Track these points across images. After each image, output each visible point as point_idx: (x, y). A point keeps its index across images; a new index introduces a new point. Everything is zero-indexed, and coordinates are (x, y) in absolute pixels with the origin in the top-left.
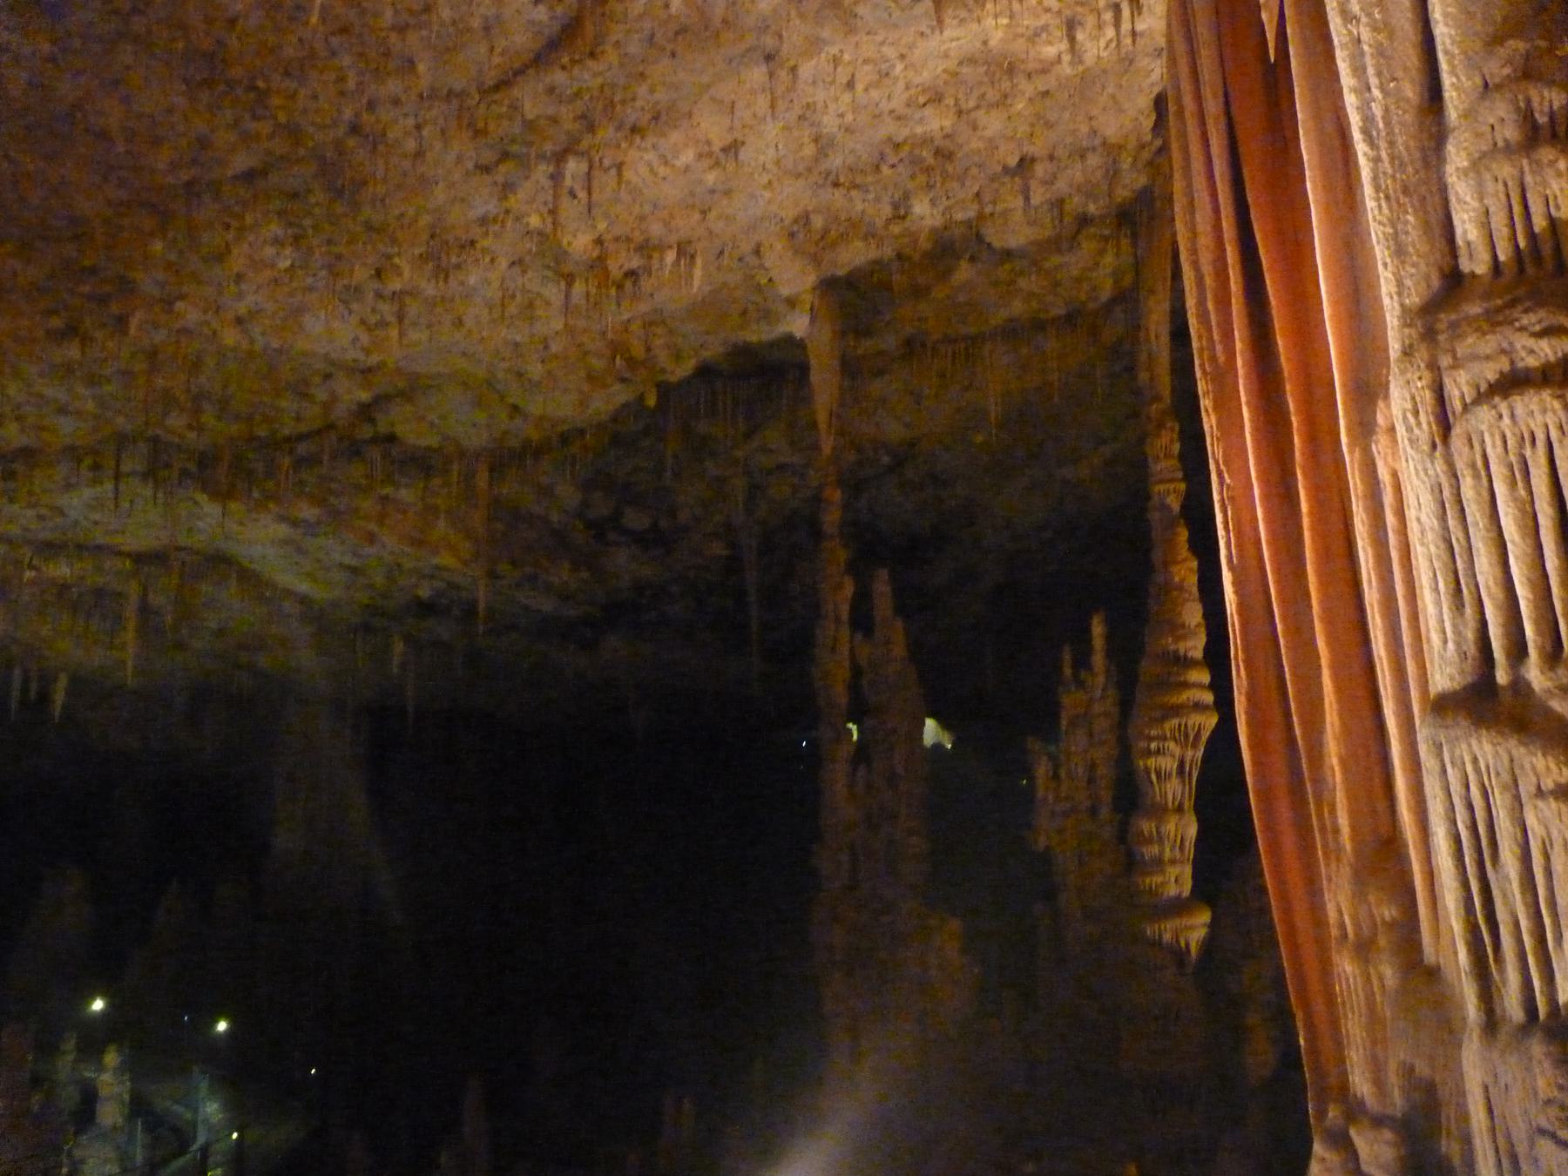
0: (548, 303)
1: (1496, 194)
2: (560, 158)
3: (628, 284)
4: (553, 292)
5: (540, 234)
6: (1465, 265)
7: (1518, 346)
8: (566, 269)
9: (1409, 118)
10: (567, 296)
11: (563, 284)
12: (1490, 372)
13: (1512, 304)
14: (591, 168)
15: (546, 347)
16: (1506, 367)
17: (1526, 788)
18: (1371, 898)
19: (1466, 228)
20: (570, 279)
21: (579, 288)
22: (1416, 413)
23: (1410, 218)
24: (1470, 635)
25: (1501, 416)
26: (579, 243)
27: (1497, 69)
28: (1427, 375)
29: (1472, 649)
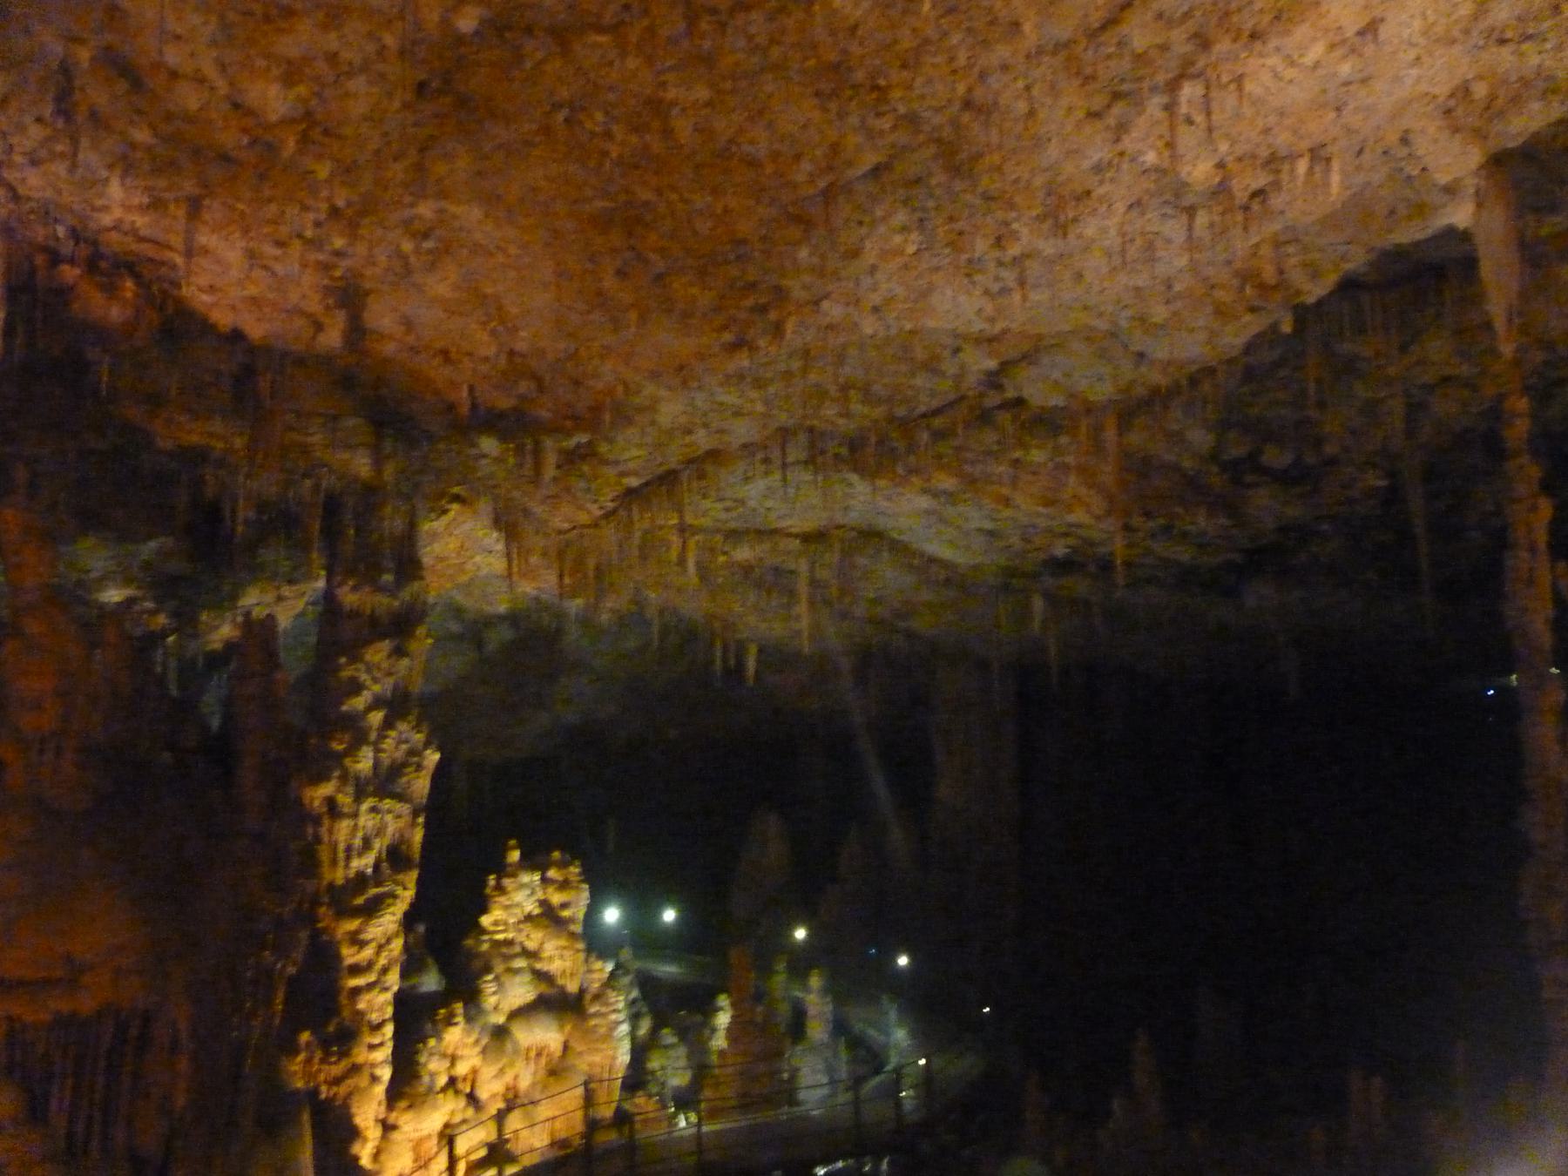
0: (1169, 241)
2: (1173, 86)
3: (1256, 206)
4: (1174, 229)
5: (1157, 169)
8: (1186, 202)
10: (1190, 228)
11: (1184, 218)
14: (1207, 88)
15: (1170, 287)
20: (1191, 211)
21: (1202, 219)
26: (1199, 171)
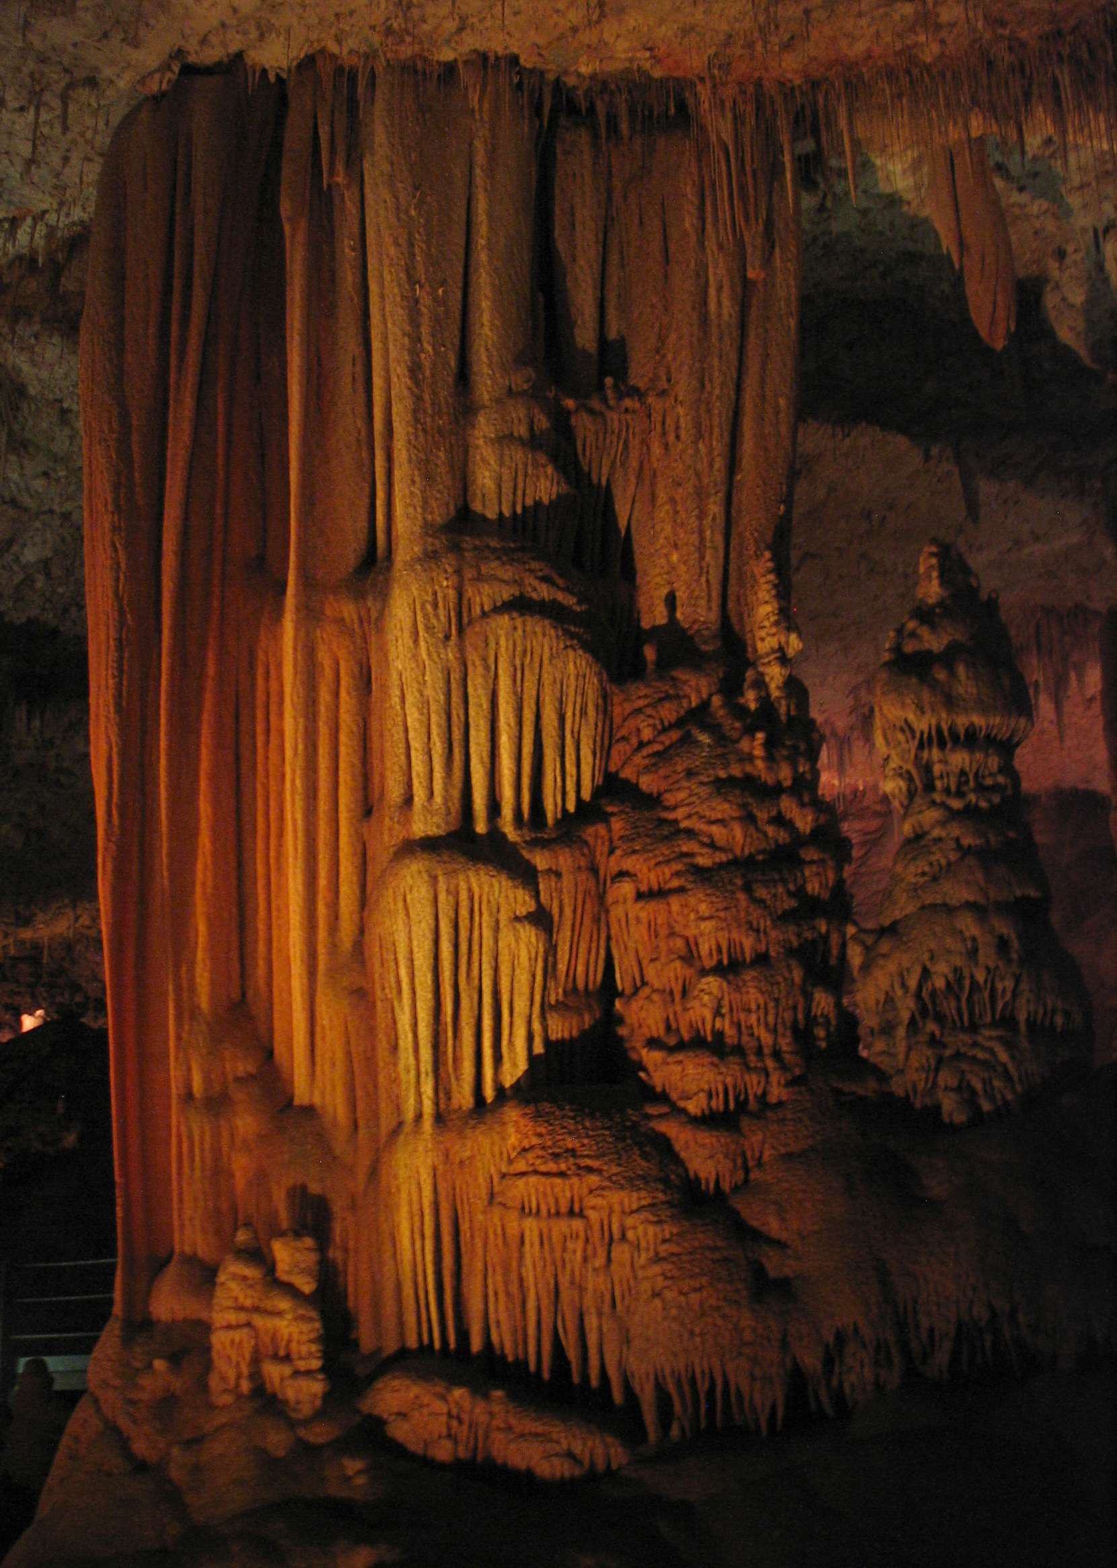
1: (510, 468)
6: (477, 507)
7: (527, 582)
9: (450, 380)
12: (506, 593)
13: (522, 549)
16: (517, 593)
17: (504, 918)
18: (227, 1054)
19: (485, 479)
22: (435, 606)
23: (441, 454)
24: (456, 793)
25: (515, 628)
27: (520, 380)
28: (454, 579)
29: (455, 805)
